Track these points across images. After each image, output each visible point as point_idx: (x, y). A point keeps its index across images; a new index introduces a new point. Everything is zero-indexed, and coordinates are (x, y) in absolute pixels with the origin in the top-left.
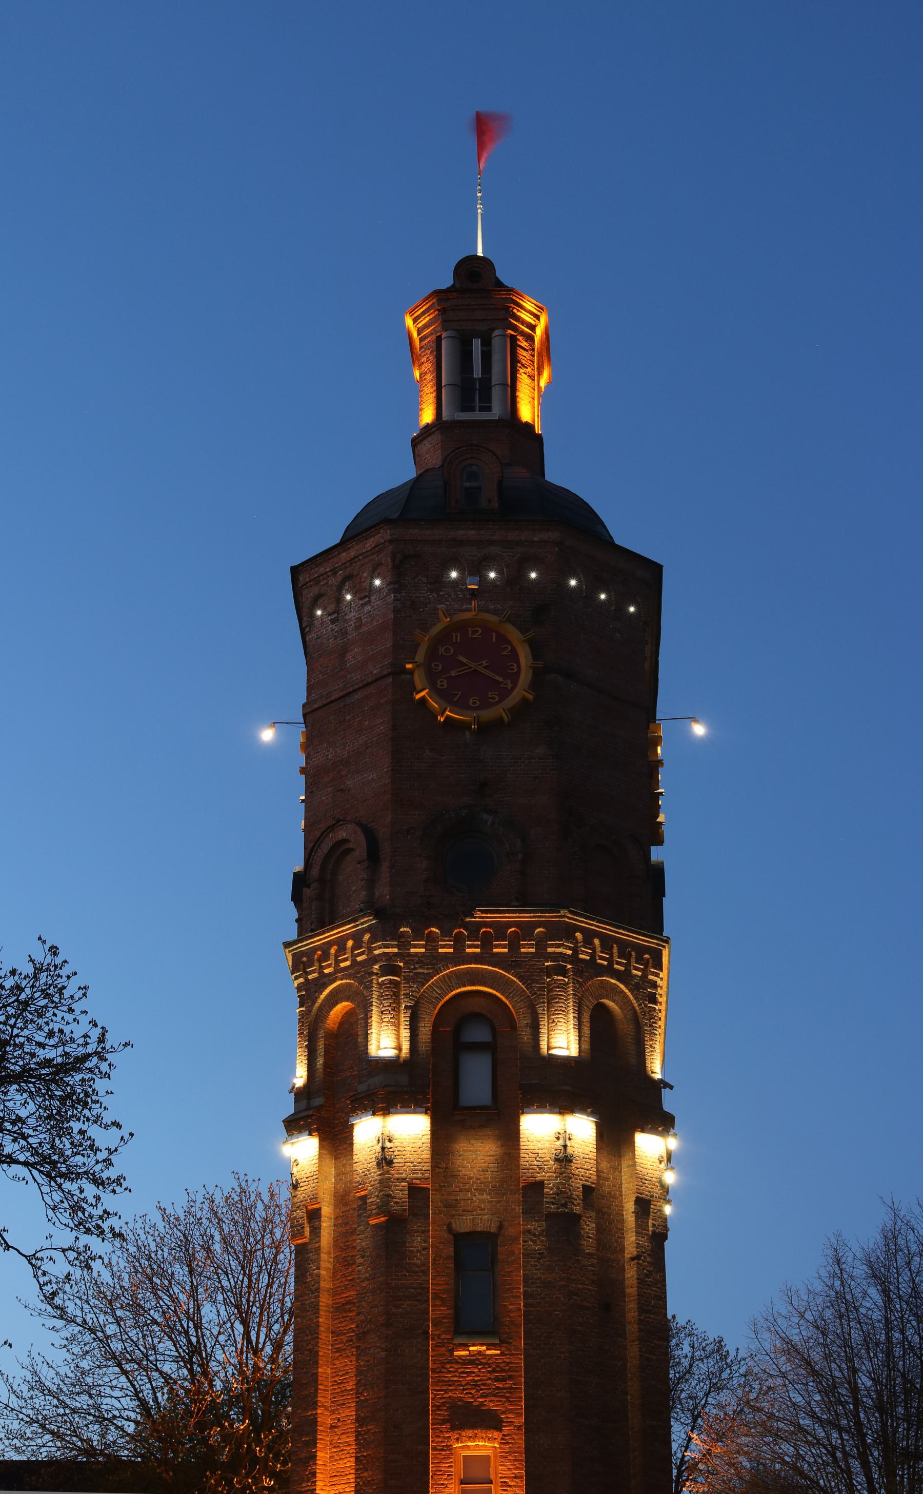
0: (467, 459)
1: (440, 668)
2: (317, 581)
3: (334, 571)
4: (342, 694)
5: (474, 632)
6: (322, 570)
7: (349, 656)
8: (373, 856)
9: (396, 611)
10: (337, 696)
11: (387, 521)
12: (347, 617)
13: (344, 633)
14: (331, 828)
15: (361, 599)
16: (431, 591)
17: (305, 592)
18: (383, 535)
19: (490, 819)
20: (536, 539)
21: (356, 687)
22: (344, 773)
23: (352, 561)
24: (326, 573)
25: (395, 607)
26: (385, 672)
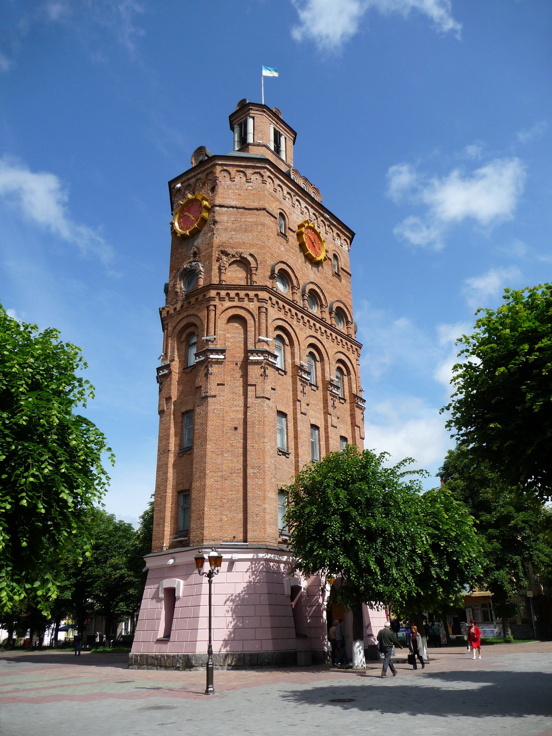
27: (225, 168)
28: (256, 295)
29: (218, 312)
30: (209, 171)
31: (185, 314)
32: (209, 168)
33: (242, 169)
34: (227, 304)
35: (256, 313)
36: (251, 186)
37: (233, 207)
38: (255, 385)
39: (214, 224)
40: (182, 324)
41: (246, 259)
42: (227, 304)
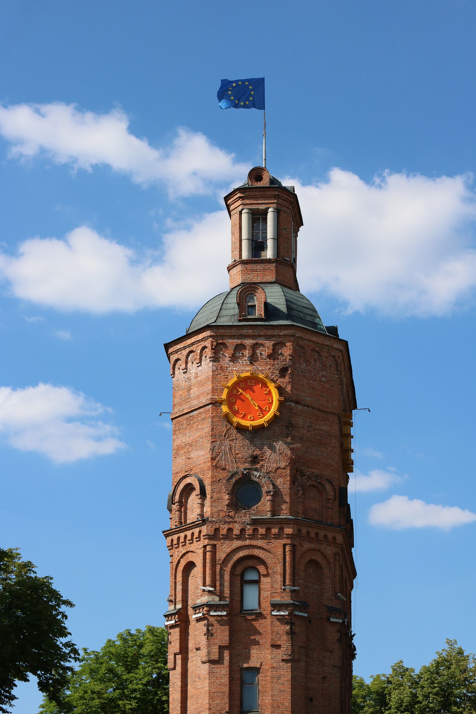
0: (249, 291)
1: (234, 400)
2: (176, 352)
3: (185, 348)
4: (189, 411)
5: (250, 382)
6: (178, 346)
7: (192, 391)
8: (203, 494)
9: (213, 371)
10: (186, 412)
11: (208, 327)
12: (191, 372)
13: (189, 379)
14: (185, 477)
15: (197, 364)
16: (229, 360)
17: (171, 356)
18: (207, 333)
19: (257, 474)
20: (282, 334)
21: (195, 408)
22: (190, 450)
23: (192, 344)
24: (180, 348)
25: (213, 369)
26: (208, 402)
27: (300, 343)
28: (334, 538)
29: (298, 555)
30: (280, 340)
31: (248, 542)
32: (280, 336)
33: (317, 349)
34: (307, 546)
35: (332, 560)
36: (325, 377)
37: (308, 407)
38: (332, 652)
39: (287, 427)
40: (241, 554)
41: (323, 486)
42: (307, 546)
